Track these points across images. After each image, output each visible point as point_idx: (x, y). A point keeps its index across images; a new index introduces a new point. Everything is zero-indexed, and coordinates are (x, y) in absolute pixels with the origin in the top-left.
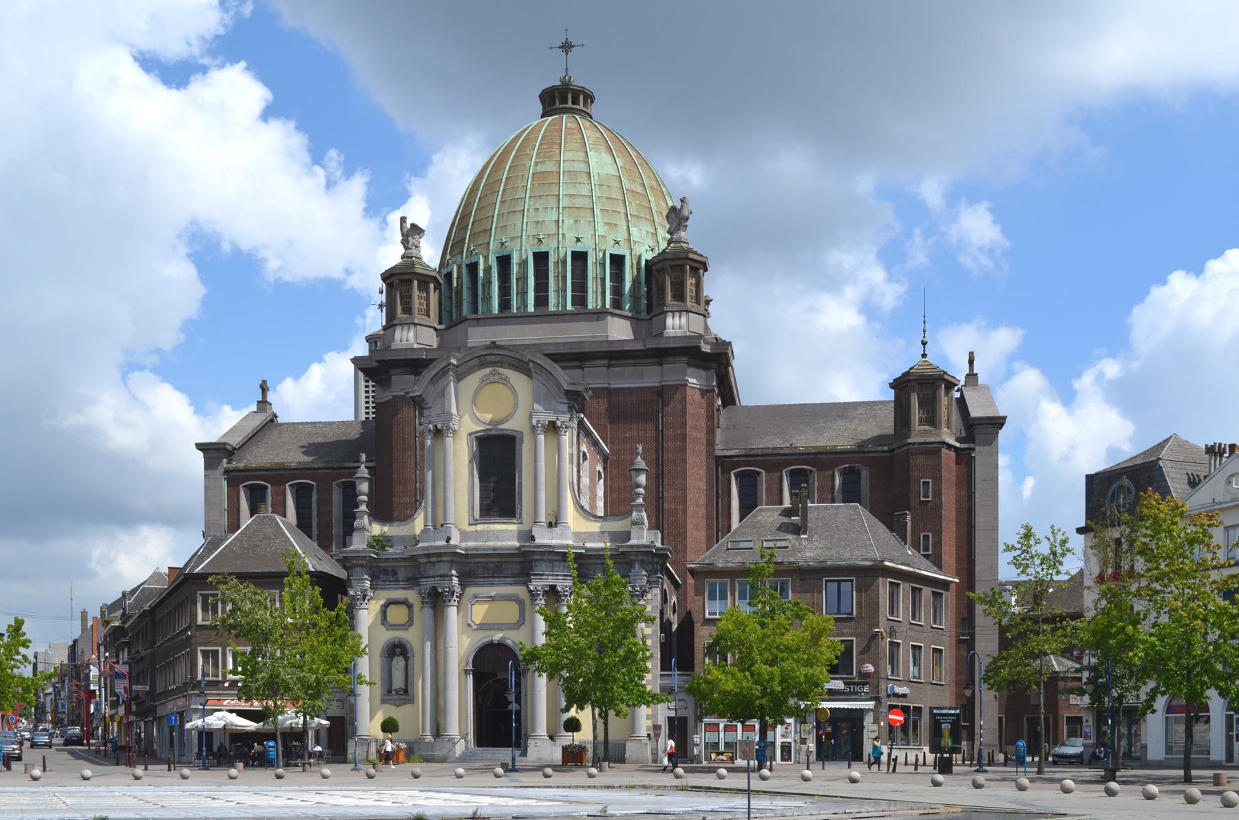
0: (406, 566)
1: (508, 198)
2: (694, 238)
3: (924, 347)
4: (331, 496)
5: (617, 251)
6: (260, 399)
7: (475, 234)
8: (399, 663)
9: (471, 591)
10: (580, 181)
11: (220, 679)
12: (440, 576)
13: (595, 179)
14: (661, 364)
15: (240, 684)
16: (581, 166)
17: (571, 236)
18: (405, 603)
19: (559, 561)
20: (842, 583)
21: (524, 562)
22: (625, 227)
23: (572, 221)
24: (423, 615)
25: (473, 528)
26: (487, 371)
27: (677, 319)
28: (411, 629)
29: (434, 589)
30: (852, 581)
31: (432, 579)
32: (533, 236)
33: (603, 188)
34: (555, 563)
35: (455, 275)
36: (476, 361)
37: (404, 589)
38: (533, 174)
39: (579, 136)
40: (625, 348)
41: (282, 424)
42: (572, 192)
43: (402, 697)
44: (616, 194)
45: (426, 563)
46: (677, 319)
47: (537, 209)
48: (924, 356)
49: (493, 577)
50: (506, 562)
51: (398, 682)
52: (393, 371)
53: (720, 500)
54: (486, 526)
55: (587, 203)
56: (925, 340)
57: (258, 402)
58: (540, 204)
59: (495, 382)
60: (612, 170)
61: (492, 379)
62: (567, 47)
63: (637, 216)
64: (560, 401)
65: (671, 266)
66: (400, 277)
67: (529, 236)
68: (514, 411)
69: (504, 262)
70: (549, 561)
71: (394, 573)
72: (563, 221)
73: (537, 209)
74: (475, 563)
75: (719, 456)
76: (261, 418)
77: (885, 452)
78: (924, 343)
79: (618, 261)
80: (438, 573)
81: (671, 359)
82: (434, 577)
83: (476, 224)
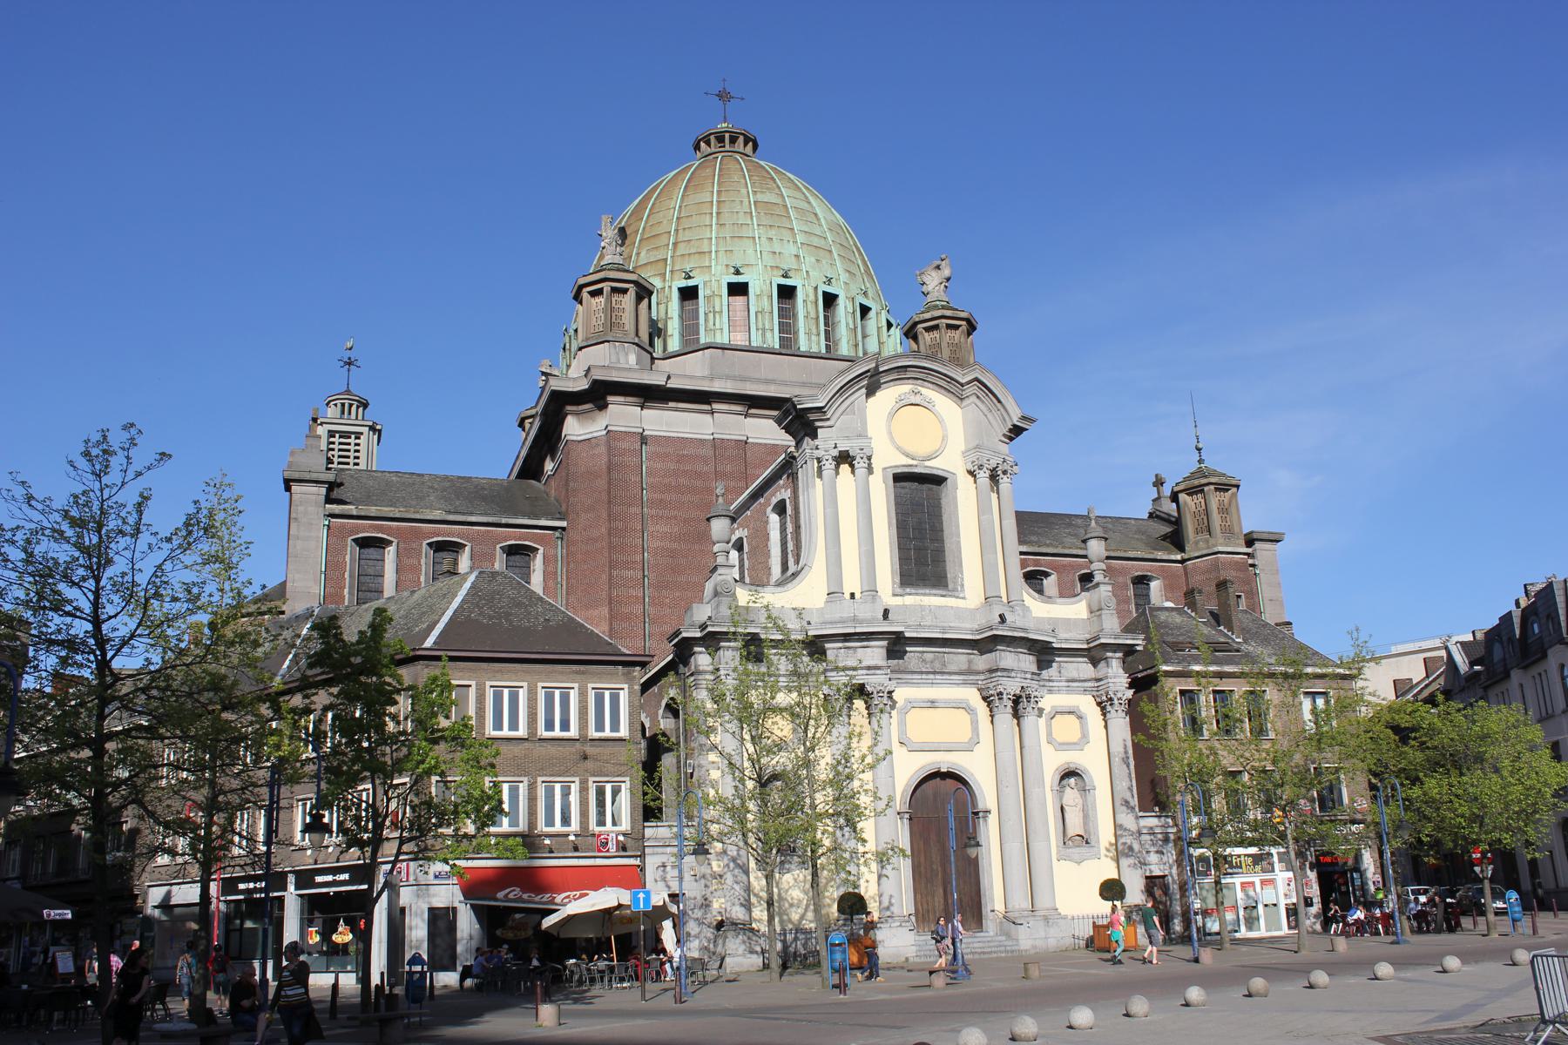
1: (726, 219)
12: (869, 668)
23: (813, 260)
25: (898, 601)
52: (610, 399)
56: (1200, 446)
58: (772, 233)
62: (723, 96)
67: (766, 266)
78: (1199, 450)
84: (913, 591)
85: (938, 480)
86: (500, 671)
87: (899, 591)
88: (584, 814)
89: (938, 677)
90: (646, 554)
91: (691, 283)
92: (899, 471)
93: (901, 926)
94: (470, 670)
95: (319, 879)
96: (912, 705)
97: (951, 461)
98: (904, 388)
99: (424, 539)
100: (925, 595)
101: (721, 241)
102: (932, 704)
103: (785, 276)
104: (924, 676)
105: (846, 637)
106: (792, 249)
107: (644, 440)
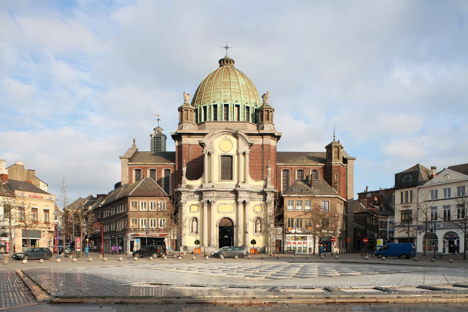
1: (215, 88)
2: (270, 102)
4: (311, 159)
5: (248, 105)
6: (133, 144)
7: (205, 98)
9: (218, 202)
10: (236, 85)
11: (137, 228)
12: (210, 197)
13: (240, 85)
15: (145, 229)
16: (236, 81)
17: (235, 100)
20: (326, 202)
22: (249, 99)
23: (235, 96)
25: (219, 183)
26: (224, 136)
30: (329, 201)
32: (224, 99)
35: (199, 110)
36: (221, 133)
38: (223, 82)
39: (234, 72)
41: (140, 152)
44: (246, 89)
47: (224, 92)
54: (223, 182)
55: (238, 91)
57: (133, 145)
58: (225, 90)
60: (245, 83)
61: (226, 139)
62: (227, 48)
69: (215, 106)
73: (224, 92)
76: (134, 151)
83: (205, 95)
84: (223, 181)
85: (231, 157)
86: (142, 199)
87: (219, 181)
88: (158, 224)
89: (227, 198)
90: (190, 170)
91: (205, 105)
94: (137, 198)
95: (121, 235)
96: (220, 204)
97: (233, 153)
101: (213, 94)
102: (225, 204)
103: (225, 102)
104: (223, 198)
105: (206, 191)
106: (230, 94)
107: (190, 145)
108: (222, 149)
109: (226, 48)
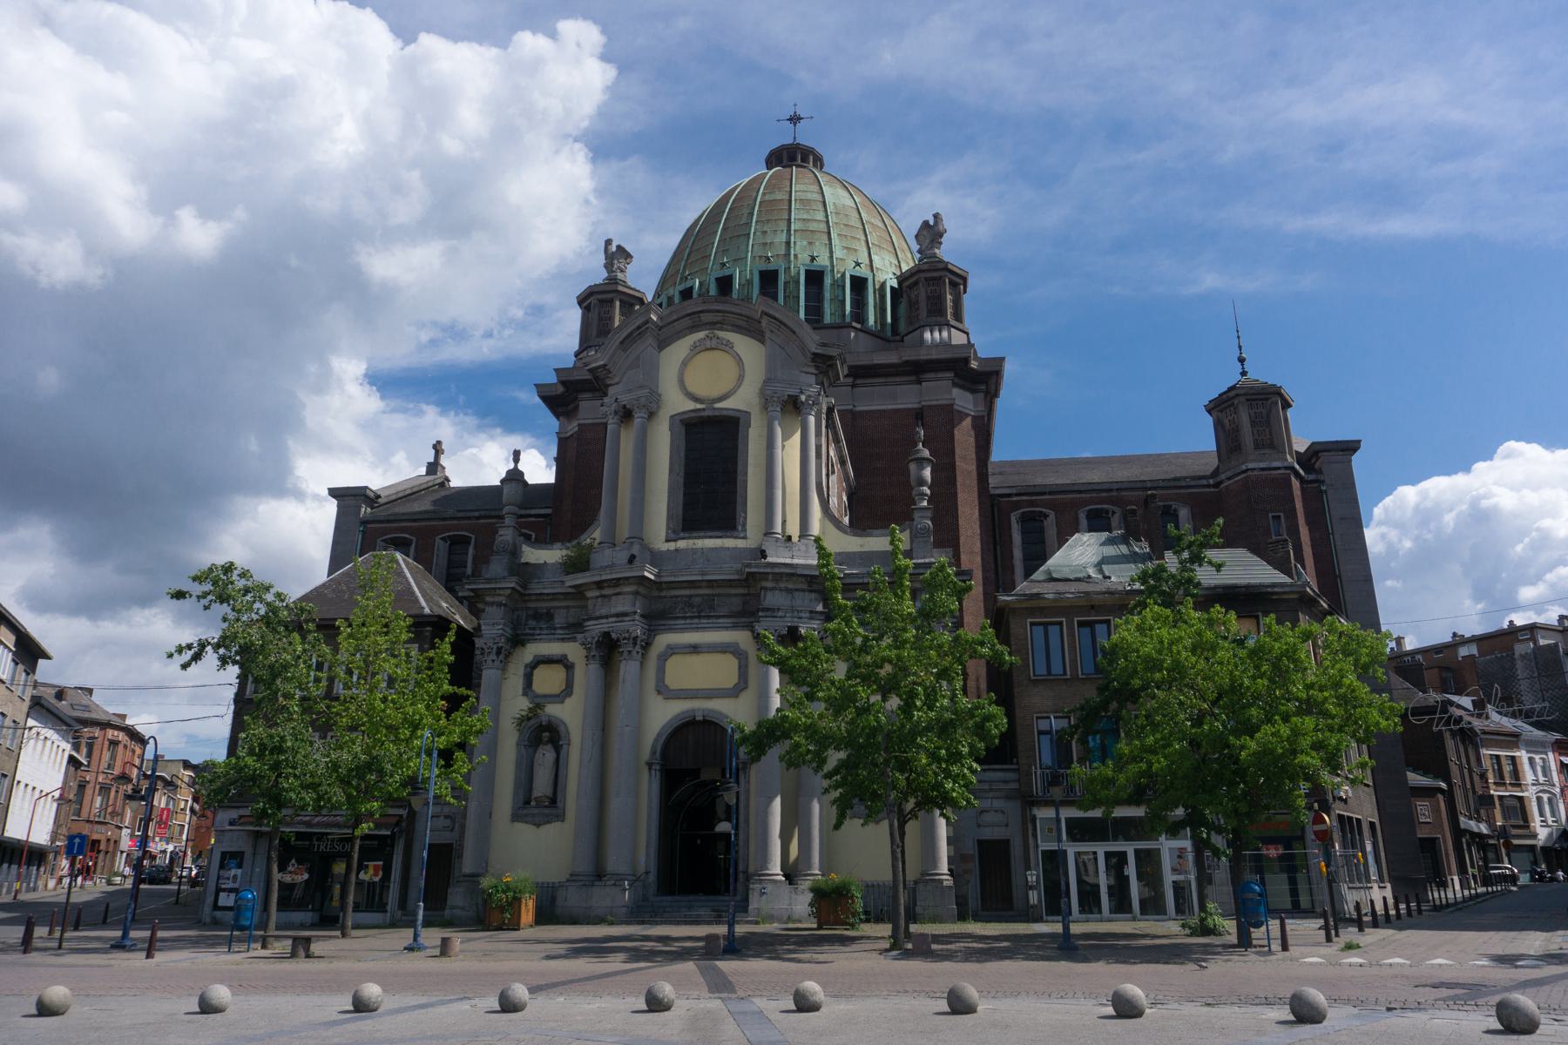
0: (568, 607)
2: (947, 251)
3: (1243, 365)
8: (546, 755)
9: (664, 640)
10: (814, 207)
12: (617, 615)
14: (919, 382)
18: (561, 661)
19: (803, 590)
21: (749, 594)
23: (805, 243)
24: (586, 675)
25: (672, 546)
27: (937, 334)
28: (568, 701)
29: (607, 635)
31: (604, 621)
33: (841, 216)
34: (797, 594)
37: (563, 640)
39: (812, 175)
40: (875, 362)
42: (805, 216)
43: (546, 811)
45: (597, 597)
46: (937, 334)
48: (1244, 373)
49: (699, 617)
50: (719, 595)
51: (542, 786)
53: (998, 547)
54: (691, 541)
59: (713, 349)
63: (879, 246)
64: (805, 369)
65: (926, 279)
66: (600, 297)
68: (741, 378)
70: (789, 591)
71: (549, 616)
72: (795, 243)
74: (672, 597)
75: (995, 495)
77: (1208, 486)
79: (859, 284)
80: (613, 611)
81: (932, 375)
82: (606, 617)
84: (687, 535)
87: (672, 536)
92: (686, 416)
93: (615, 885)
96: (672, 650)
97: (744, 400)
98: (701, 335)
99: (439, 534)
100: (699, 538)
102: (695, 649)
104: (688, 621)
108: (691, 389)
109: (790, 119)
